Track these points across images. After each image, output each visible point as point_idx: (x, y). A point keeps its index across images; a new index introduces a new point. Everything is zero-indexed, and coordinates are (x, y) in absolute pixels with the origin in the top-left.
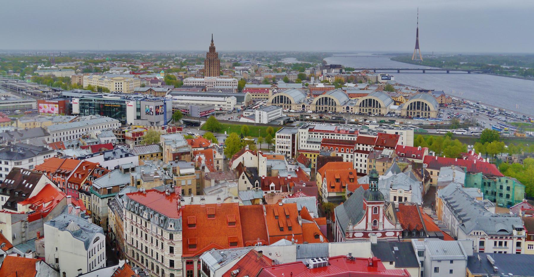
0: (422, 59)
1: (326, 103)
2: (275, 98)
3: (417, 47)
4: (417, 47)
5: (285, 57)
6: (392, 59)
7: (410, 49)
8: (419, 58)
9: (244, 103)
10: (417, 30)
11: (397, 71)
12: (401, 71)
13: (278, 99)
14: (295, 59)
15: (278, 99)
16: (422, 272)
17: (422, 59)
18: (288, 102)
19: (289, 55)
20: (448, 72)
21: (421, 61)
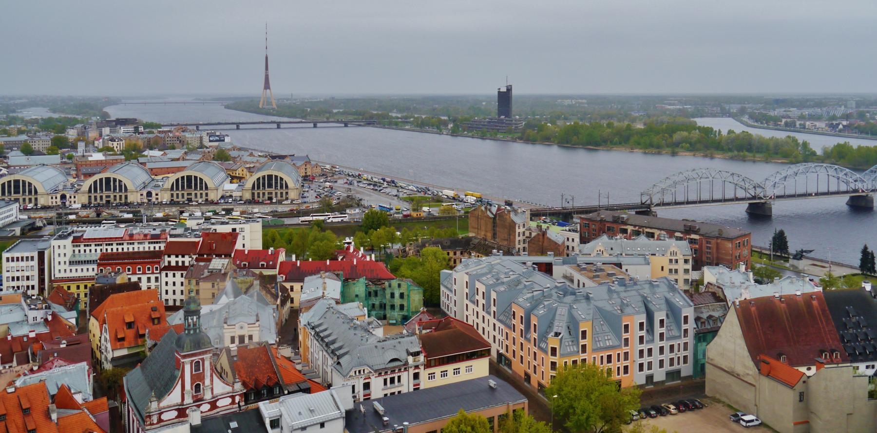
0: (275, 106)
1: (270, 186)
3: (267, 86)
4: (267, 86)
5: (24, 106)
6: (227, 107)
7: (255, 89)
8: (269, 103)
11: (235, 126)
12: (241, 126)
14: (46, 109)
16: (801, 395)
17: (275, 106)
19: (34, 103)
20: (315, 126)
21: (273, 109)
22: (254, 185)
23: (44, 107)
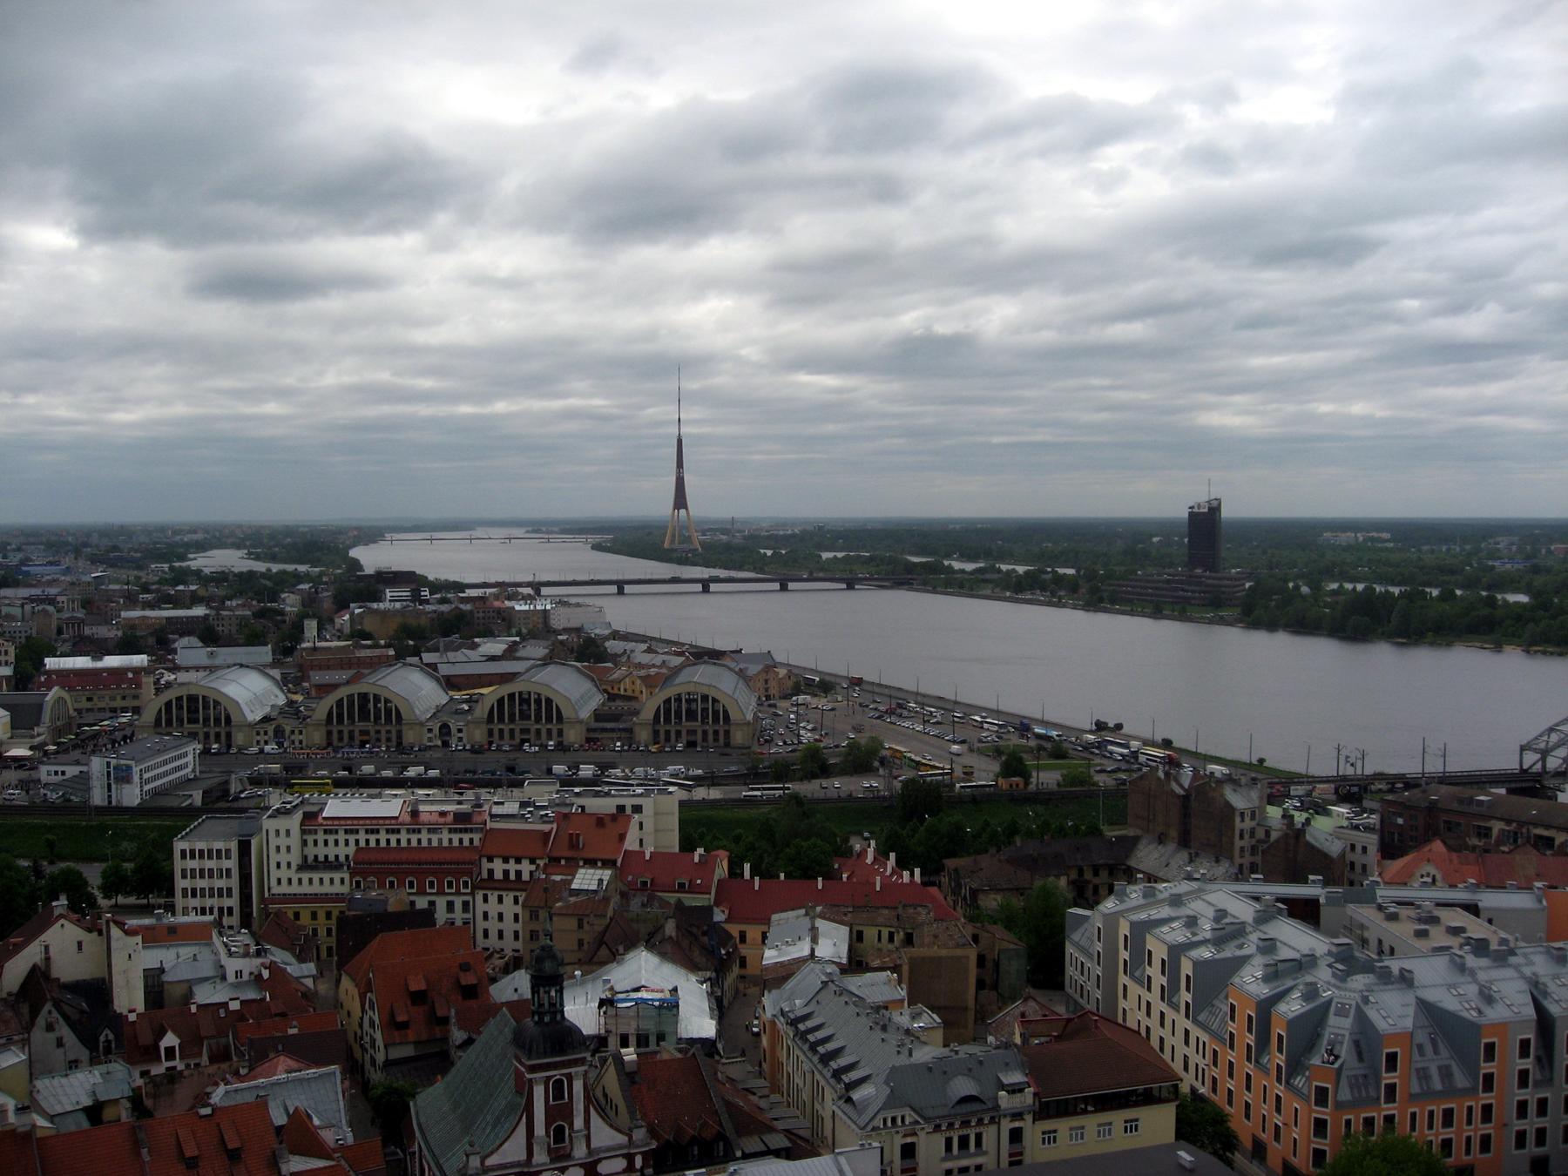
1: (364, 715)
2: (168, 704)
3: (680, 501)
4: (680, 501)
5: (201, 547)
6: (597, 547)
8: (688, 539)
9: (42, 732)
10: (680, 442)
11: (614, 589)
12: (627, 588)
13: (180, 708)
15: (180, 708)
18: (217, 721)
19: (216, 538)
20: (784, 588)
22: (330, 714)
23: (238, 547)
